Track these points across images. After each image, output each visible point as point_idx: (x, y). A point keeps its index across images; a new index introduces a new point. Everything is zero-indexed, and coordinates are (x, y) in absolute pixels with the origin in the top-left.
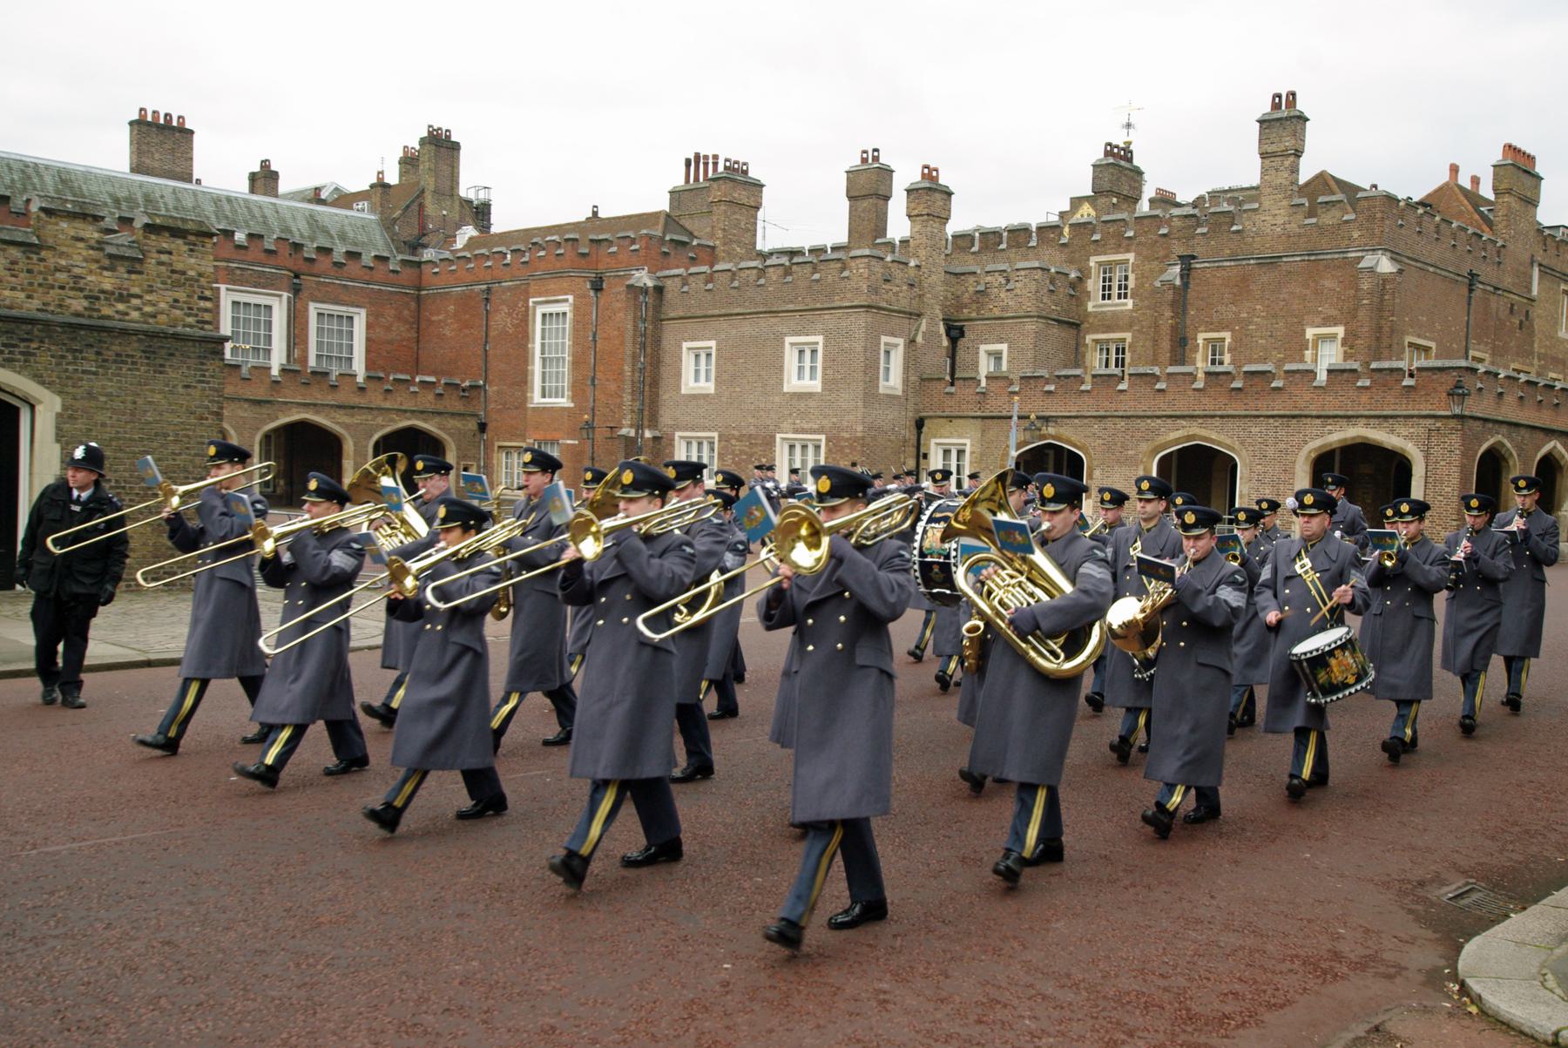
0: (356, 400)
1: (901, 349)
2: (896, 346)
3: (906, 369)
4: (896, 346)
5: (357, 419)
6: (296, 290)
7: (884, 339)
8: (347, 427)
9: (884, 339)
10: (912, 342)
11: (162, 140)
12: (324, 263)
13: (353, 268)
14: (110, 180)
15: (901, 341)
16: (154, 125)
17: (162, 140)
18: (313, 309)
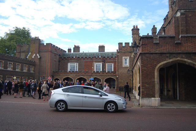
0: (102, 75)
1: (128, 58)
2: (127, 58)
3: (130, 62)
4: (127, 58)
5: (102, 77)
6: (105, 62)
7: (123, 57)
8: (101, 78)
9: (123, 57)
10: (130, 57)
11: (102, 48)
12: (108, 59)
13: (112, 59)
14: (97, 53)
15: (128, 57)
16: (101, 47)
17: (102, 48)
18: (107, 64)
